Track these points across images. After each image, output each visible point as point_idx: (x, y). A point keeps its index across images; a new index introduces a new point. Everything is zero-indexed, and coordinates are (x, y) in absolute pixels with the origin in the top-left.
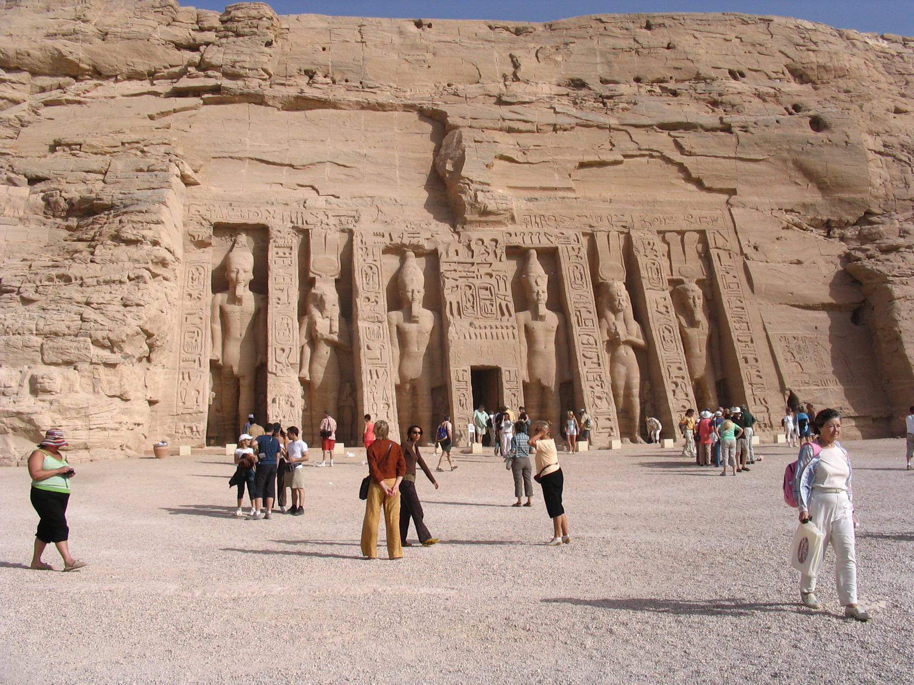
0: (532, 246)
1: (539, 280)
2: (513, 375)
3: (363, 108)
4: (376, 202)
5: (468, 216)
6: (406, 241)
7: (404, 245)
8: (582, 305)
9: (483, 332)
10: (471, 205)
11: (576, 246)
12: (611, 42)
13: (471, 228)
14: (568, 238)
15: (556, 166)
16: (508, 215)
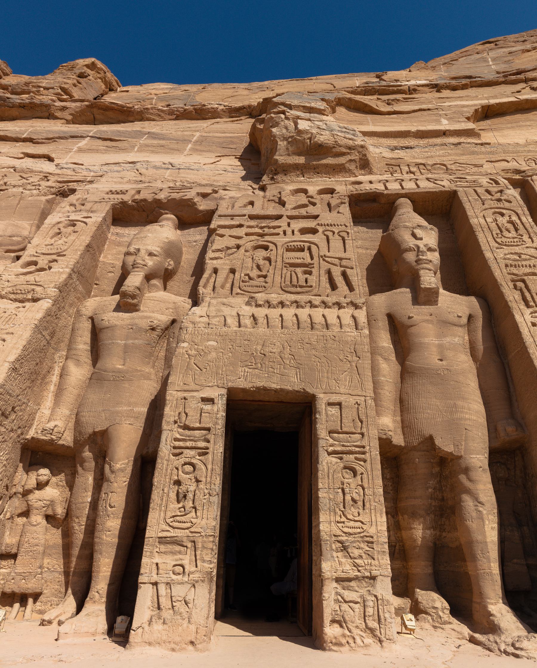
0: (403, 192)
1: (418, 232)
2: (349, 414)
3: (177, 118)
4: (138, 166)
5: (282, 158)
6: (162, 196)
7: (157, 202)
8: (528, 270)
9: (274, 313)
10: (285, 139)
11: (494, 189)
12: (507, 50)
13: (286, 178)
14: (474, 181)
15: (441, 112)
16: (355, 156)
